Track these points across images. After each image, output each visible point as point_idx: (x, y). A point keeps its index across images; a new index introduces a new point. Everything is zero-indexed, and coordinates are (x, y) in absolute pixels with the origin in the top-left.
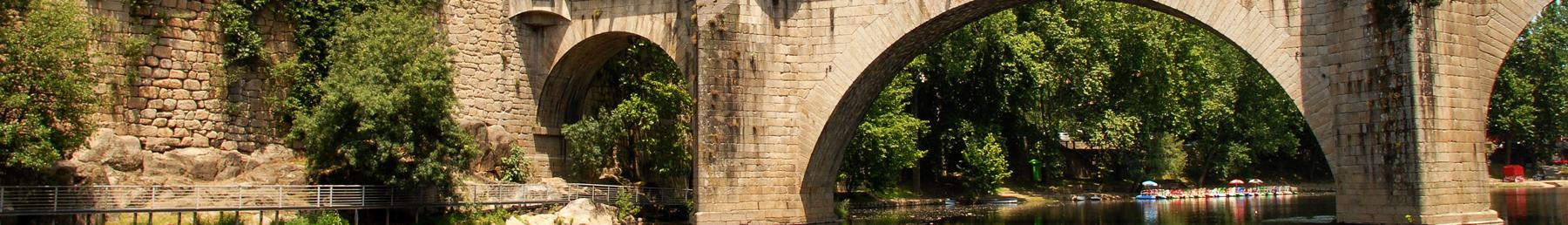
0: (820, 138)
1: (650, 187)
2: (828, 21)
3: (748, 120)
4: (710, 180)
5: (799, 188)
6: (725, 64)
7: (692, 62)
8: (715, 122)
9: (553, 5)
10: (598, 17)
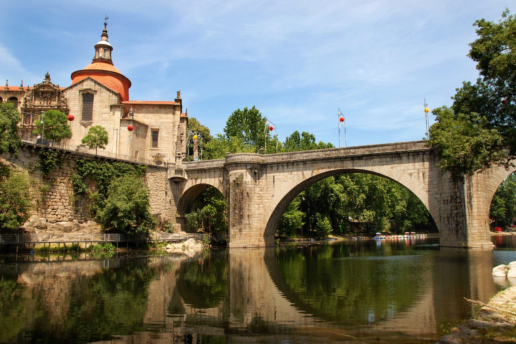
0: (270, 219)
1: (214, 234)
2: (272, 180)
3: (246, 213)
4: (234, 232)
5: (263, 235)
6: (239, 194)
7: (228, 194)
8: (235, 213)
9: (182, 175)
10: (197, 179)
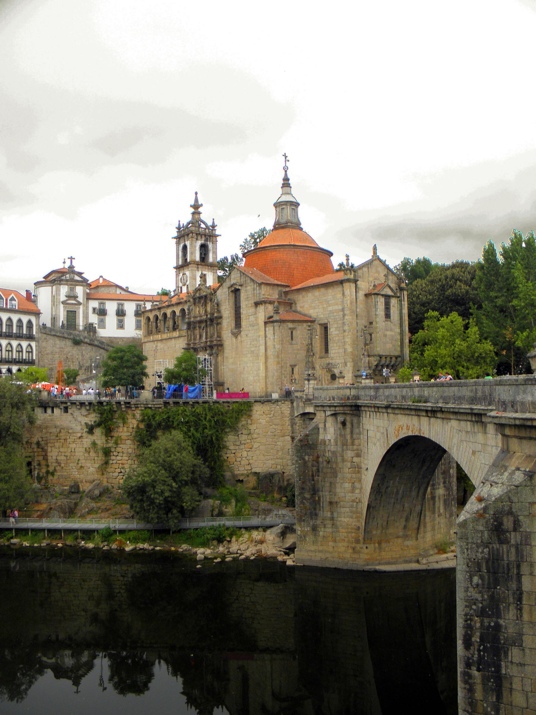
3: (325, 496)
4: (302, 531)
6: (310, 464)
8: (304, 498)
